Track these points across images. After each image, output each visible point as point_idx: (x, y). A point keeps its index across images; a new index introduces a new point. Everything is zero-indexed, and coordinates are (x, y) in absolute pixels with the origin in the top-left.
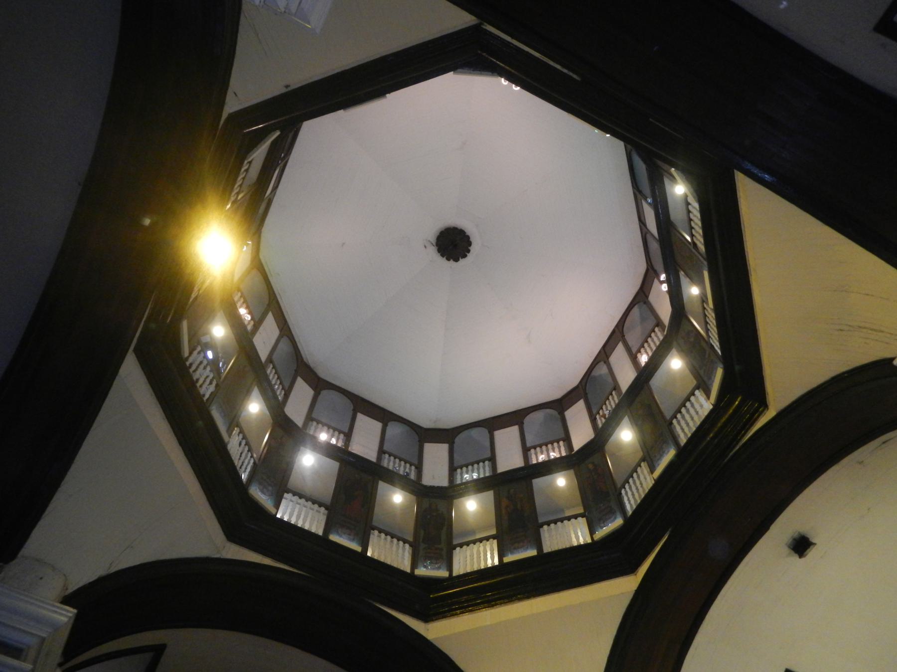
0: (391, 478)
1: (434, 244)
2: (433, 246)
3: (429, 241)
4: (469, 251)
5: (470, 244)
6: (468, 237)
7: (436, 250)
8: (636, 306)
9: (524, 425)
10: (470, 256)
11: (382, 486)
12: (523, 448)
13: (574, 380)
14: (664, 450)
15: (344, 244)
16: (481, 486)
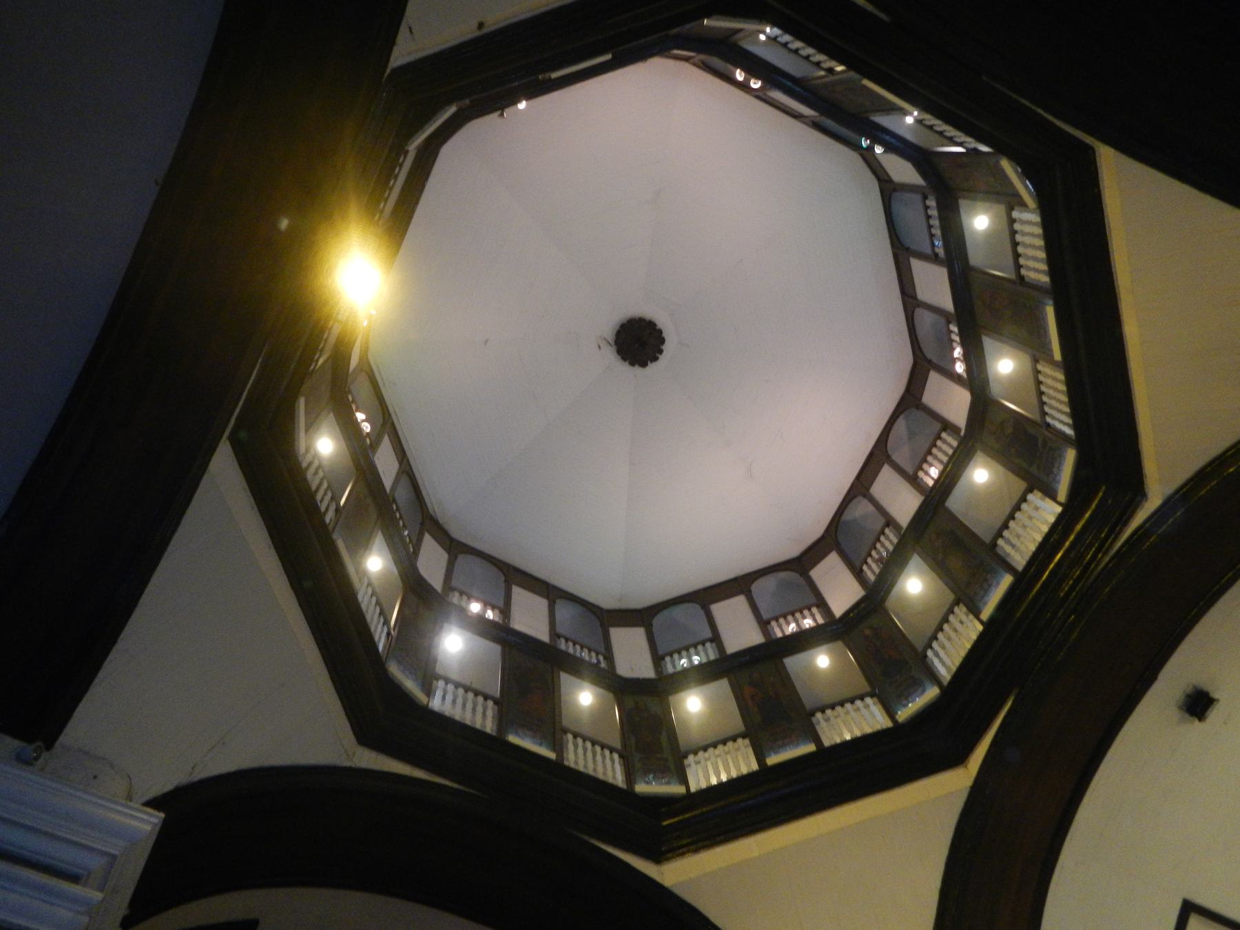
0: (575, 667)
1: (612, 342)
2: (611, 346)
3: (605, 339)
4: (661, 352)
5: (662, 341)
6: (660, 332)
7: (615, 351)
8: (901, 417)
9: (753, 593)
10: (664, 359)
11: (565, 679)
12: (759, 622)
13: (815, 527)
14: (990, 582)
15: (487, 341)
16: (706, 674)
